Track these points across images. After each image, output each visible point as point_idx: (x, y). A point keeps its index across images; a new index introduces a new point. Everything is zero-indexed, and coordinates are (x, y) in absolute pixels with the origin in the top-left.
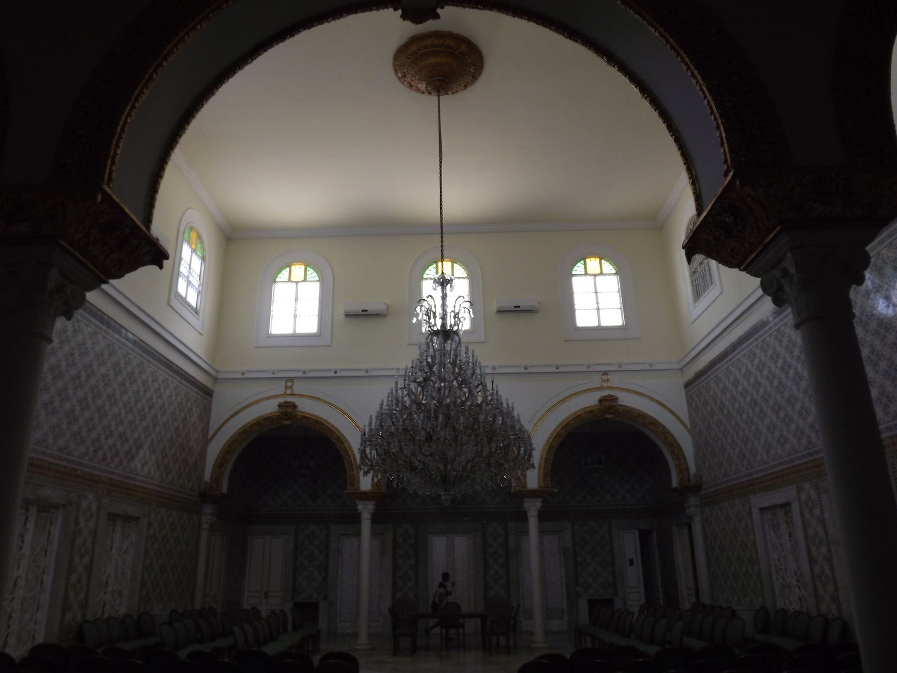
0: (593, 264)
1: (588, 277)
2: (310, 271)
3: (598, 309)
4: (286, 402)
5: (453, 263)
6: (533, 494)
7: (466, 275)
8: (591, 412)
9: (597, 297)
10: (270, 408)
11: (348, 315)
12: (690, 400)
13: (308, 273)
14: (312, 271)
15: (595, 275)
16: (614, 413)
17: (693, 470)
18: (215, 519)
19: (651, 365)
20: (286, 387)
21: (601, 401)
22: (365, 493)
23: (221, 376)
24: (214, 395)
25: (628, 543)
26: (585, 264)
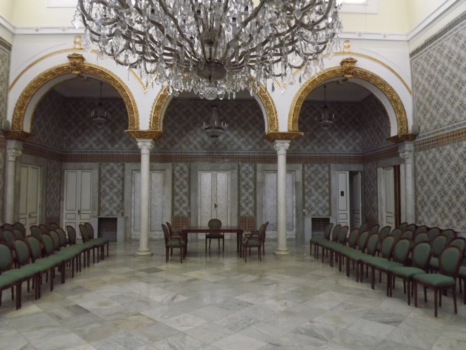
4: (74, 54)
6: (284, 136)
8: (334, 71)
10: (62, 60)
12: (414, 69)
16: (352, 74)
18: (20, 153)
20: (75, 42)
21: (342, 63)
22: (143, 132)
23: (17, 32)
24: (13, 48)
25: (341, 180)
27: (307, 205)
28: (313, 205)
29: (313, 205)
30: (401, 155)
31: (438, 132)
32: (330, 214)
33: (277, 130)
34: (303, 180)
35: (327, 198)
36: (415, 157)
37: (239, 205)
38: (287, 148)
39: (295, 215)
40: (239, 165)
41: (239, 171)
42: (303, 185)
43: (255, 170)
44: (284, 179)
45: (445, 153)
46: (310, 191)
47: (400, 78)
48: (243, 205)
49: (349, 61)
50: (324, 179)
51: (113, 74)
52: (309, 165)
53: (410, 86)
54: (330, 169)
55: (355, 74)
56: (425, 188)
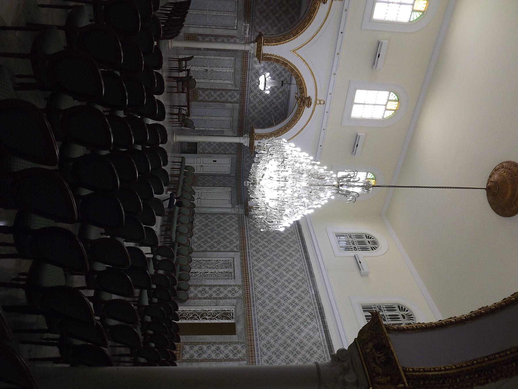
2: (418, 15)
7: (385, 117)
11: (379, 44)
13: (418, 13)
14: (418, 16)
30: (237, 206)
31: (247, 229)
32: (200, 153)
35: (212, 152)
36: (235, 214)
37: (207, 89)
40: (237, 90)
41: (234, 90)
43: (234, 102)
45: (234, 232)
48: (207, 93)
51: (309, 26)
54: (232, 154)
56: (216, 220)
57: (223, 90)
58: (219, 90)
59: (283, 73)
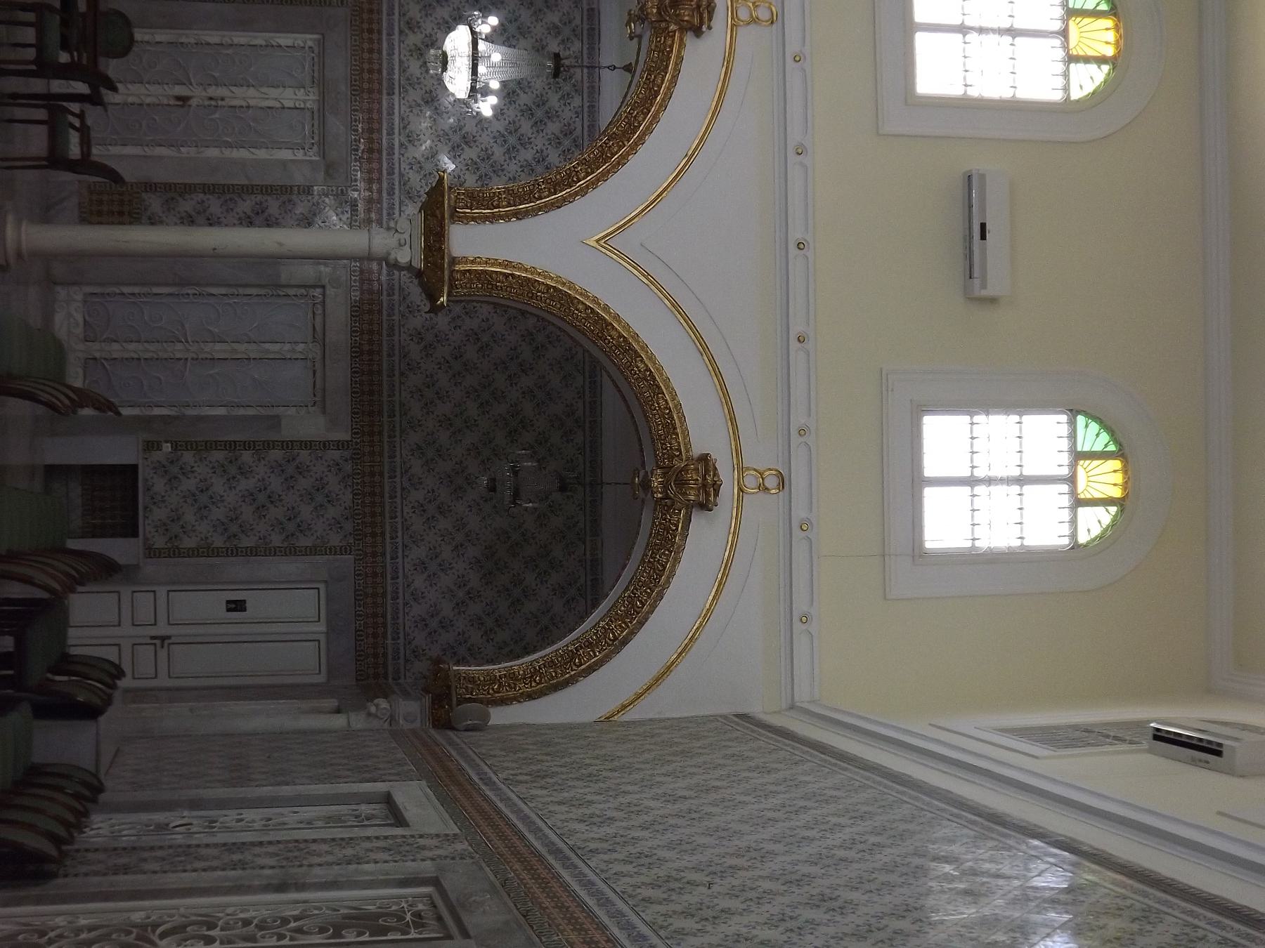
0: (1105, 479)
1: (1065, 459)
3: (971, 482)
5: (1112, 61)
8: (671, 428)
9: (1008, 481)
15: (1071, 480)
17: (499, 716)
19: (805, 618)
26: (1103, 455)
27: (188, 457)
28: (190, 484)
29: (190, 484)
33: (456, 217)
34: (287, 445)
35: (218, 542)
38: (392, 257)
39: (148, 412)
42: (269, 445)
44: (280, 244)
46: (244, 472)
47: (658, 680)
49: (709, 479)
50: (291, 527)
52: (348, 467)
53: (632, 715)
54: (332, 551)
55: (666, 505)
57: (268, 190)
58: (248, 190)
59: (554, 100)
